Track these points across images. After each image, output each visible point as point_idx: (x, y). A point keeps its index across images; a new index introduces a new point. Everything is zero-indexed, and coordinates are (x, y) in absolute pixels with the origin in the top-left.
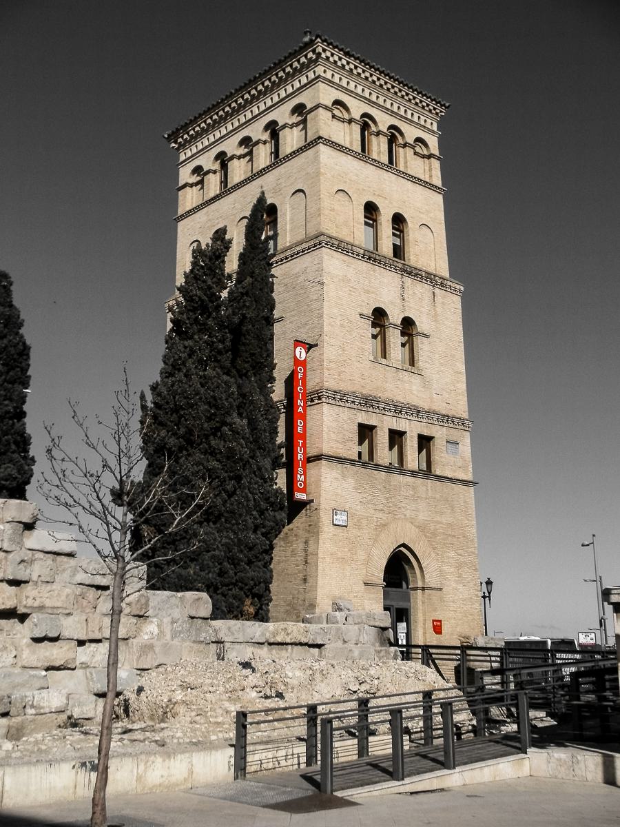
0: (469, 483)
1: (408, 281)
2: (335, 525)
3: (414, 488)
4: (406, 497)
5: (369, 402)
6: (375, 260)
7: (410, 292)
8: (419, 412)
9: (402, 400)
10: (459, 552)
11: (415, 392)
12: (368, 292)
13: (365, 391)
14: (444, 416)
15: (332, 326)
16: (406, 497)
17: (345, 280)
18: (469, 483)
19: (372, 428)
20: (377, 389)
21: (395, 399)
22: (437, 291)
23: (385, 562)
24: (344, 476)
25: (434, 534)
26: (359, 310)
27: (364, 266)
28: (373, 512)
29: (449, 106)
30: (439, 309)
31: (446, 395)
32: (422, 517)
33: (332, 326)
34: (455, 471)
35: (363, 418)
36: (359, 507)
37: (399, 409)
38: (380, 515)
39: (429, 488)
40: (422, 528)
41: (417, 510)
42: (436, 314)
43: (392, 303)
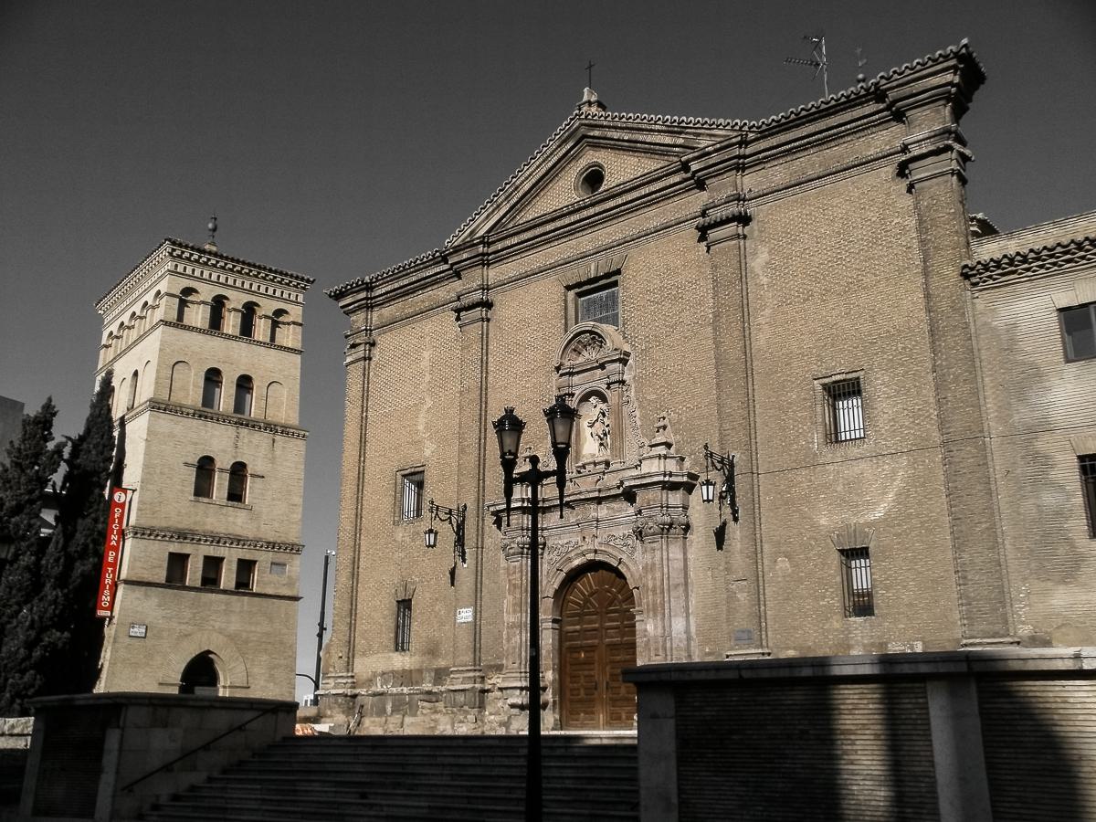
0: (301, 325)
1: (244, 431)
2: (130, 636)
3: (227, 604)
4: (216, 612)
5: (182, 535)
6: (206, 417)
7: (246, 441)
8: (240, 540)
9: (224, 531)
10: (274, 656)
11: (239, 524)
12: (196, 444)
13: (180, 526)
14: (269, 543)
15: (151, 474)
16: (216, 612)
17: (172, 435)
18: (301, 325)
19: (185, 557)
20: (195, 523)
21: (215, 531)
22: (278, 438)
23: (184, 666)
24: (146, 596)
25: (246, 642)
26: (184, 460)
27: (196, 423)
28: (176, 625)
29: (314, 280)
30: (278, 452)
31: (276, 525)
32: (234, 626)
33: (151, 474)
34: (277, 588)
35: (175, 548)
36: (160, 621)
37: (216, 539)
38: (183, 627)
39: (245, 603)
40: (232, 638)
41: (229, 622)
42: (274, 458)
43: (224, 451)
